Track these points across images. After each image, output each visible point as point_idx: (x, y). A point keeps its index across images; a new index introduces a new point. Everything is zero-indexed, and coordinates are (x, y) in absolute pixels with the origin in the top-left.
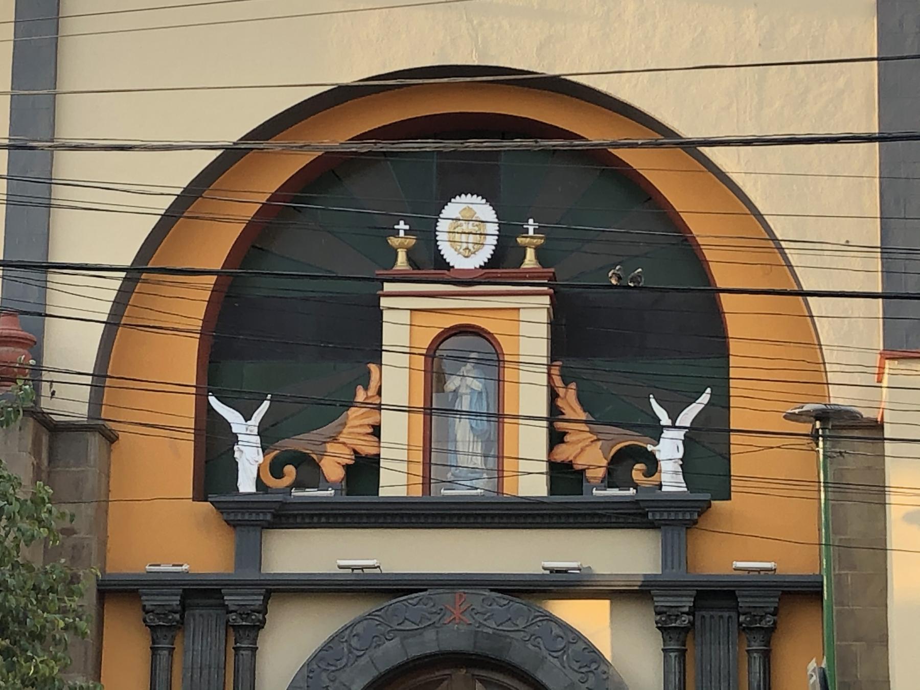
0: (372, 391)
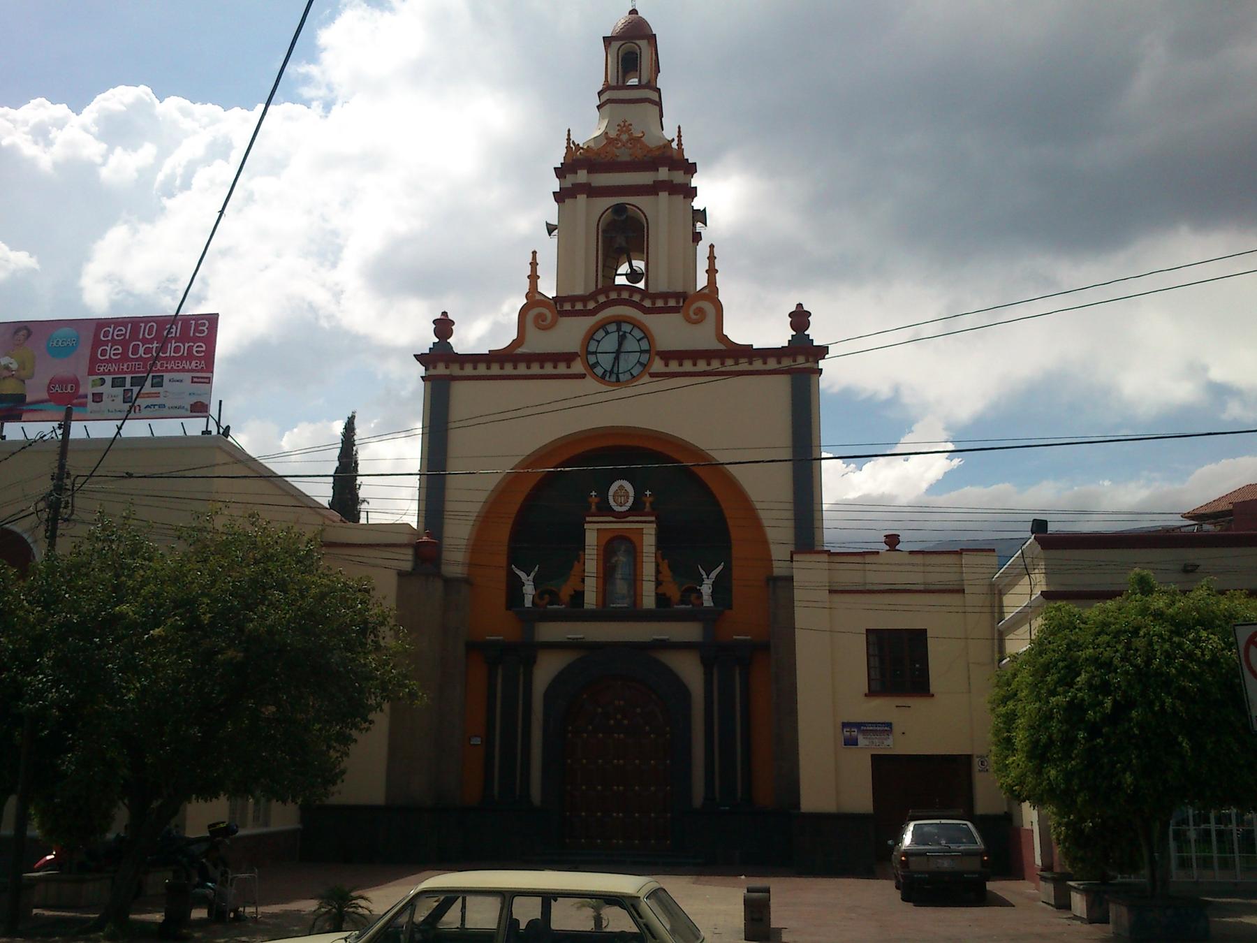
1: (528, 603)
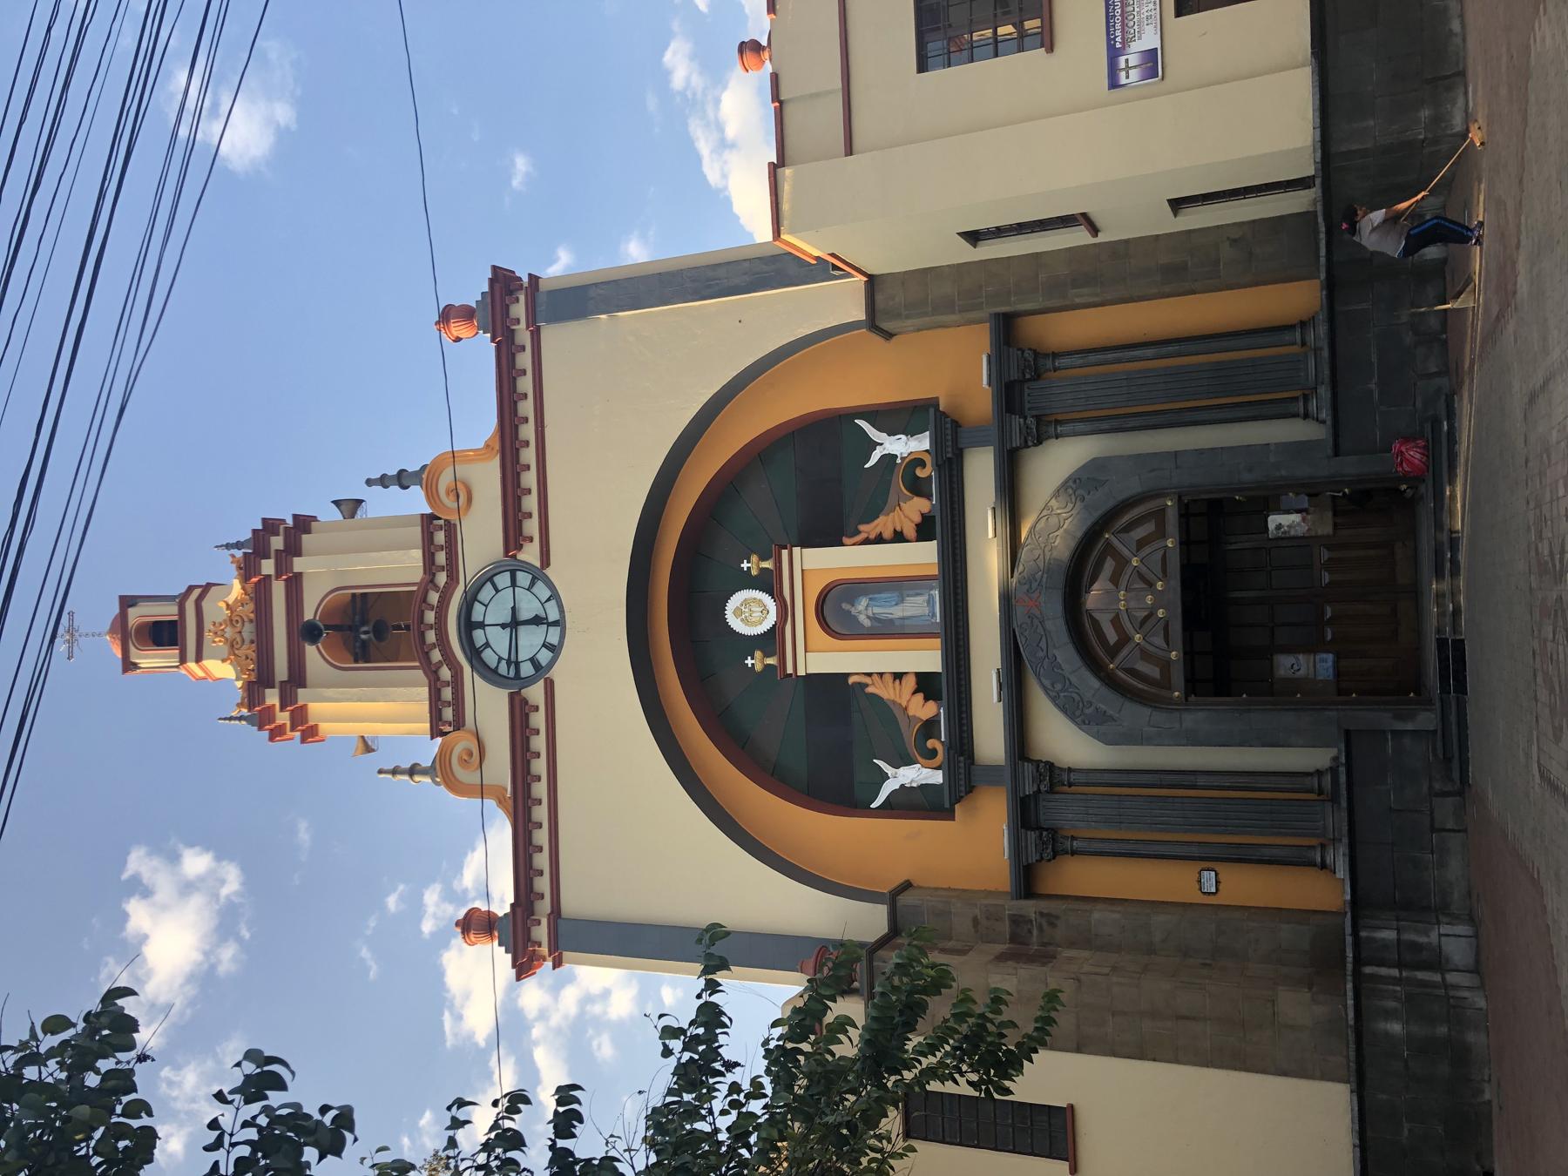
0: (867, 680)
1: (937, 777)
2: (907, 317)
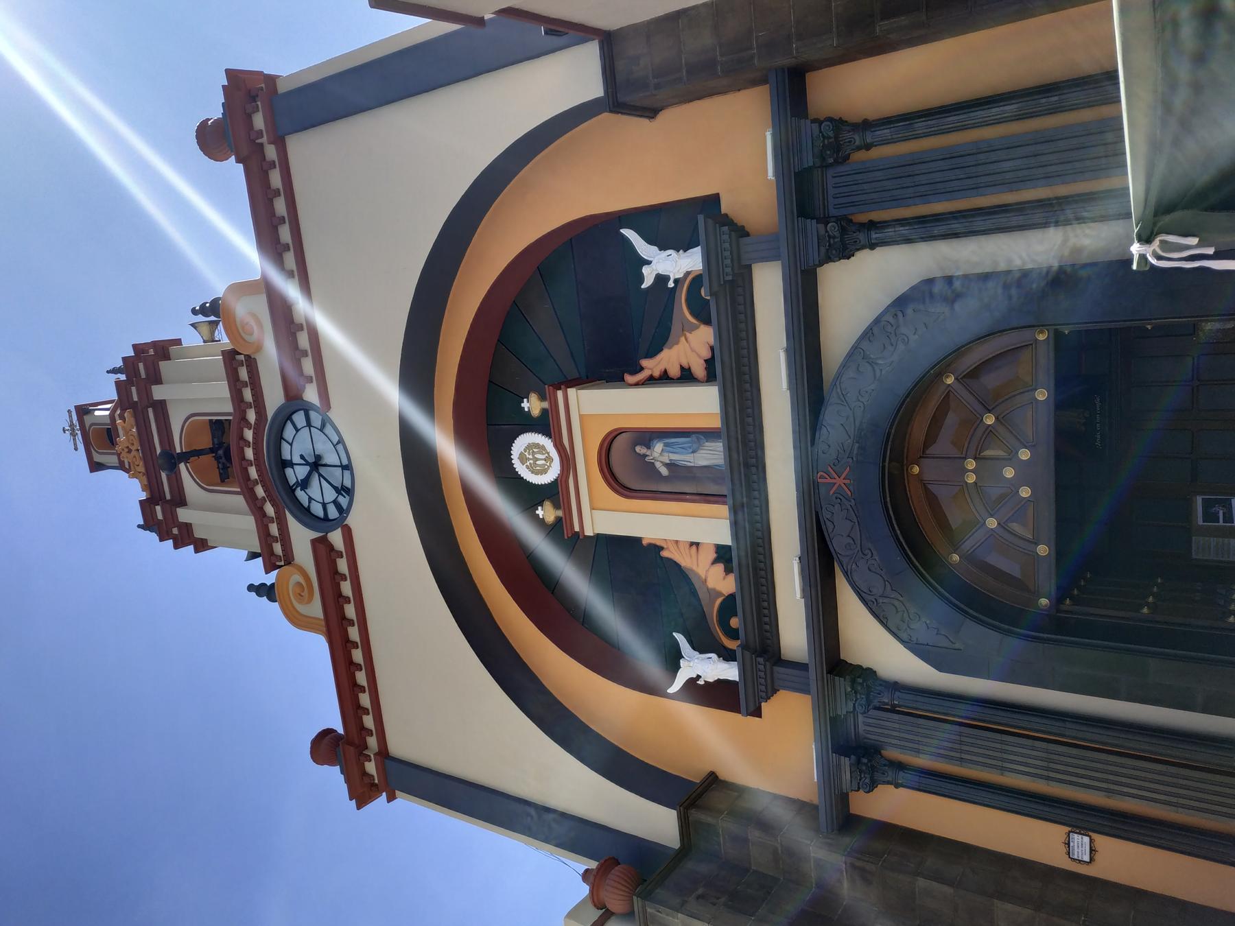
2: (658, 86)
